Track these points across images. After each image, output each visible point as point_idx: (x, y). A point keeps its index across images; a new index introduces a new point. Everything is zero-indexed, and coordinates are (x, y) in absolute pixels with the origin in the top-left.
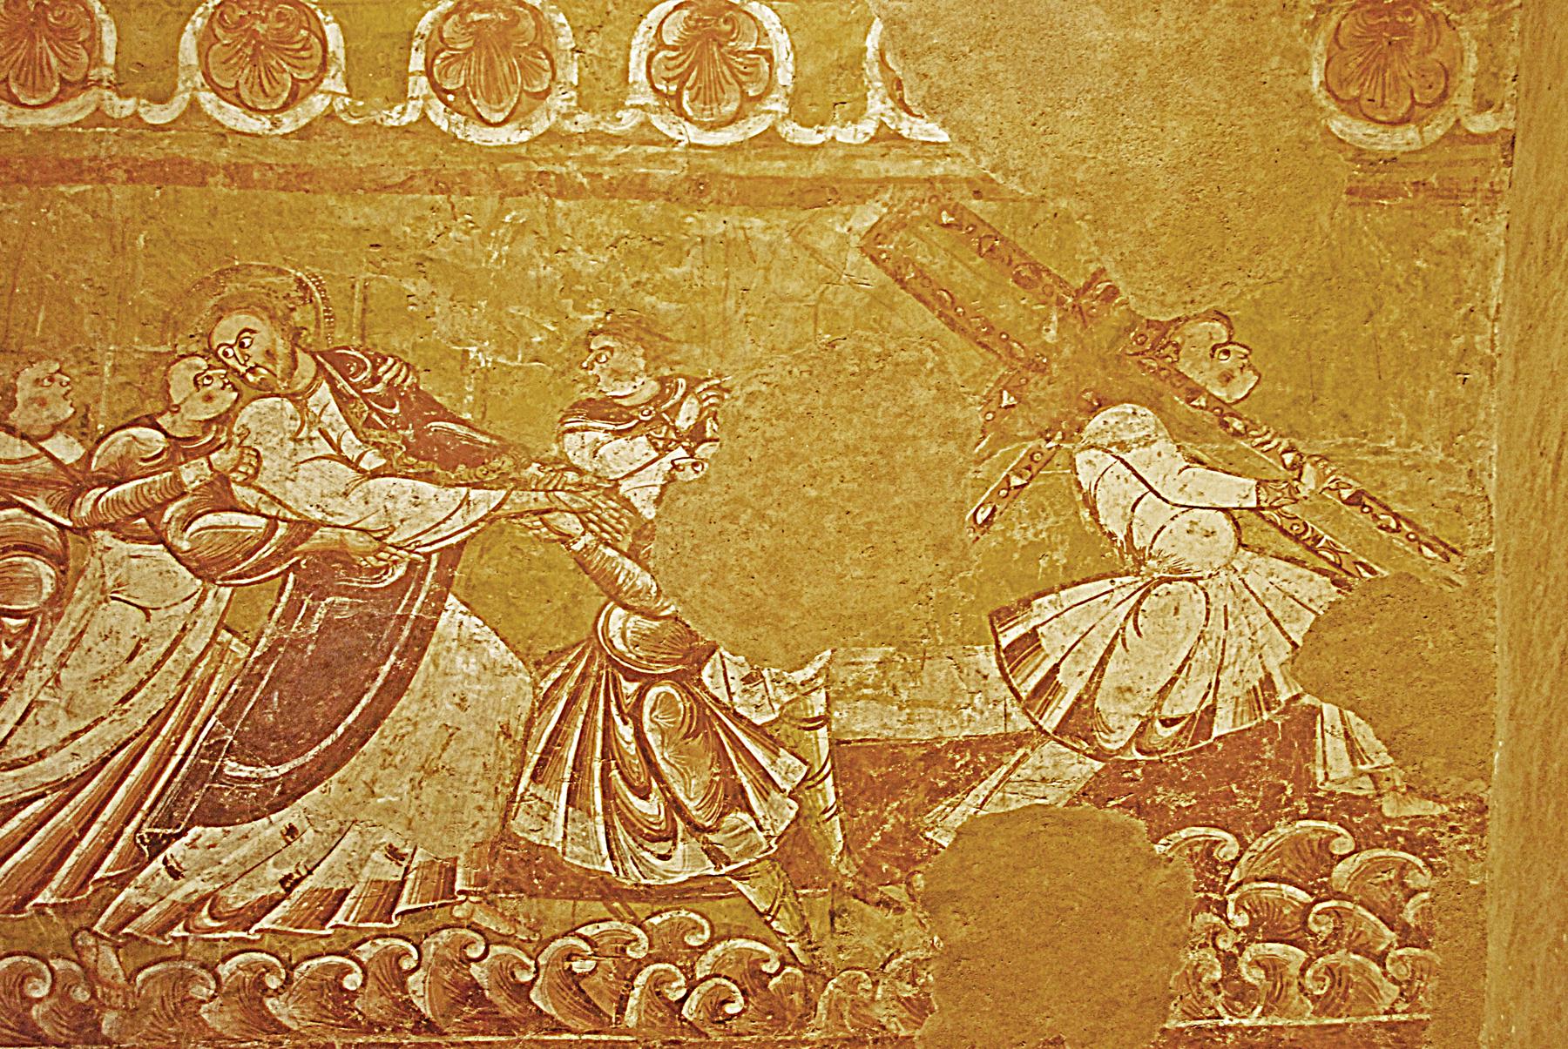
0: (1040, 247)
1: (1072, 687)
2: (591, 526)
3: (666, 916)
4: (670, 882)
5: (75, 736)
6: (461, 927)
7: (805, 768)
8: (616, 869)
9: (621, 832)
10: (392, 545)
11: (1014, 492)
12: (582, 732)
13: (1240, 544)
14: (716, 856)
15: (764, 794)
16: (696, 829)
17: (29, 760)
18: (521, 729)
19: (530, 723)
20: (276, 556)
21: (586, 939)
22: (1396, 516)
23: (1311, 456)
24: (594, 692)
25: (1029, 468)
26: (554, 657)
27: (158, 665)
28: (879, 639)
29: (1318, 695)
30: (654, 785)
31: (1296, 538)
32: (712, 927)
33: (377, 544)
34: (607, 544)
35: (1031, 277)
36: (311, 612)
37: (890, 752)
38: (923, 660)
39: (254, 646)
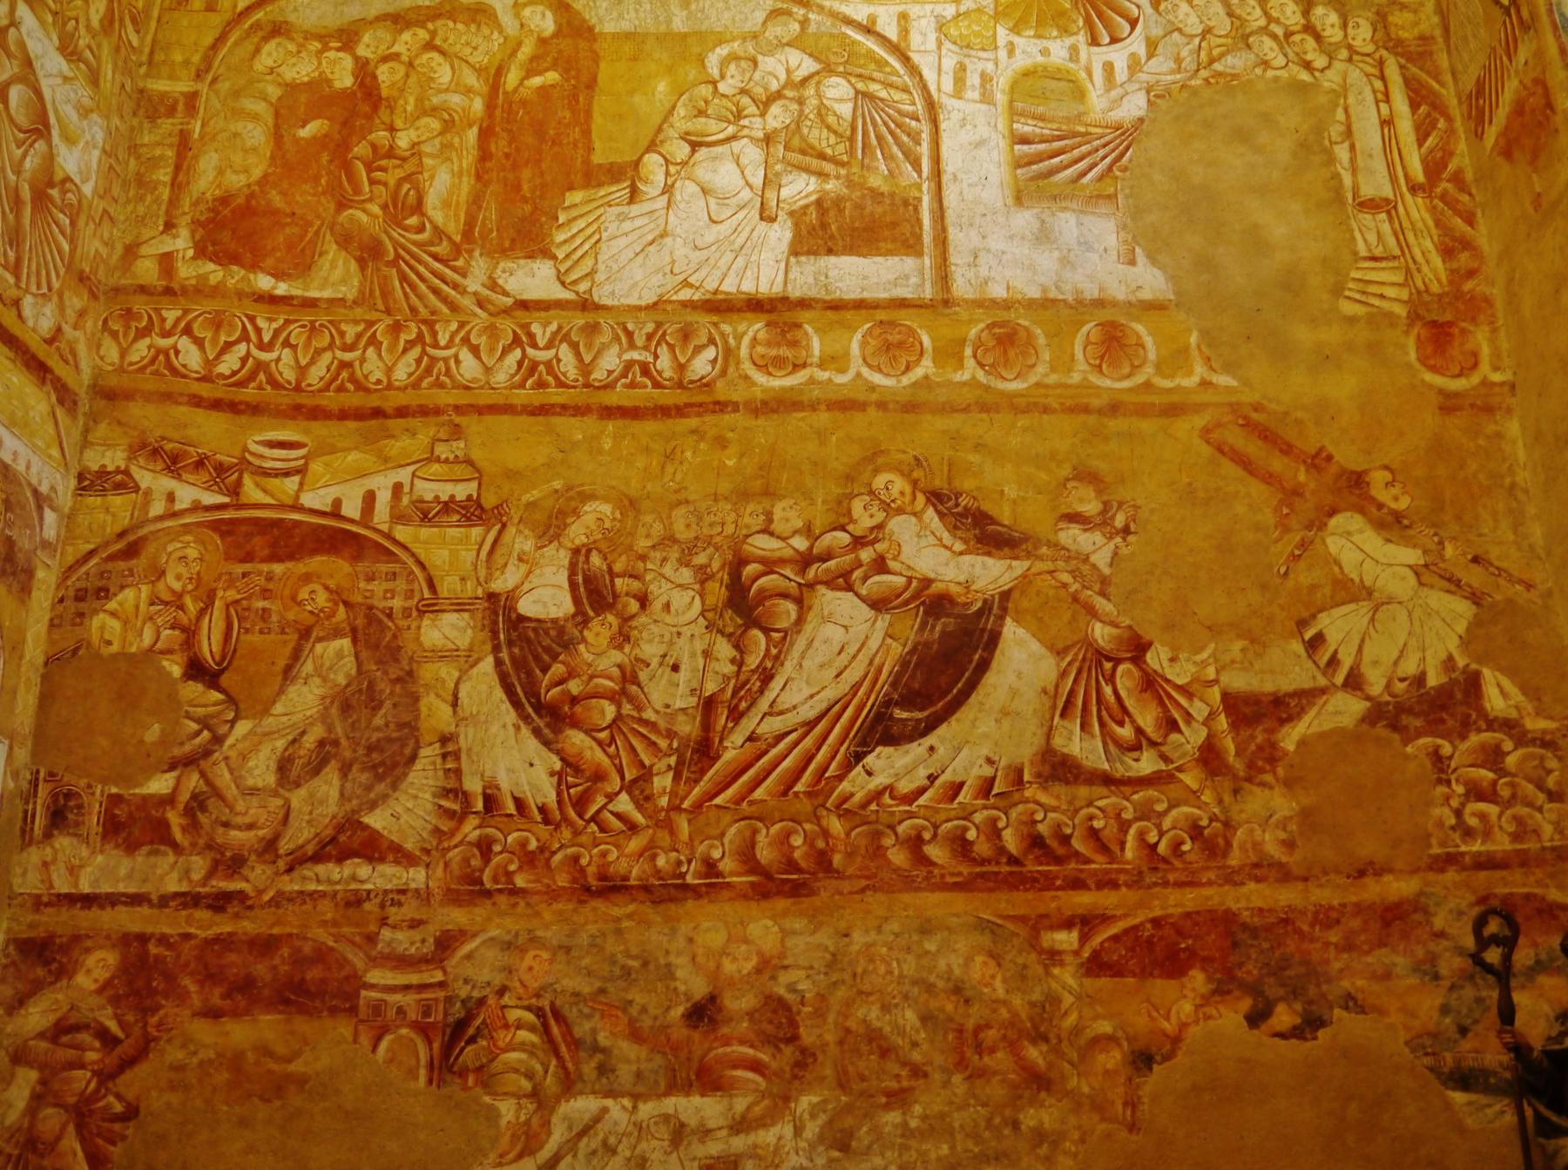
0: (1290, 434)
1: (1347, 661)
5: (812, 696)
9: (1112, 748)
13: (1421, 584)
14: (1165, 759)
16: (1153, 744)
17: (788, 711)
19: (1057, 686)
20: (913, 598)
27: (854, 657)
28: (1240, 636)
29: (1479, 660)
31: (1449, 580)
35: (1287, 449)
36: (933, 627)
37: (1253, 700)
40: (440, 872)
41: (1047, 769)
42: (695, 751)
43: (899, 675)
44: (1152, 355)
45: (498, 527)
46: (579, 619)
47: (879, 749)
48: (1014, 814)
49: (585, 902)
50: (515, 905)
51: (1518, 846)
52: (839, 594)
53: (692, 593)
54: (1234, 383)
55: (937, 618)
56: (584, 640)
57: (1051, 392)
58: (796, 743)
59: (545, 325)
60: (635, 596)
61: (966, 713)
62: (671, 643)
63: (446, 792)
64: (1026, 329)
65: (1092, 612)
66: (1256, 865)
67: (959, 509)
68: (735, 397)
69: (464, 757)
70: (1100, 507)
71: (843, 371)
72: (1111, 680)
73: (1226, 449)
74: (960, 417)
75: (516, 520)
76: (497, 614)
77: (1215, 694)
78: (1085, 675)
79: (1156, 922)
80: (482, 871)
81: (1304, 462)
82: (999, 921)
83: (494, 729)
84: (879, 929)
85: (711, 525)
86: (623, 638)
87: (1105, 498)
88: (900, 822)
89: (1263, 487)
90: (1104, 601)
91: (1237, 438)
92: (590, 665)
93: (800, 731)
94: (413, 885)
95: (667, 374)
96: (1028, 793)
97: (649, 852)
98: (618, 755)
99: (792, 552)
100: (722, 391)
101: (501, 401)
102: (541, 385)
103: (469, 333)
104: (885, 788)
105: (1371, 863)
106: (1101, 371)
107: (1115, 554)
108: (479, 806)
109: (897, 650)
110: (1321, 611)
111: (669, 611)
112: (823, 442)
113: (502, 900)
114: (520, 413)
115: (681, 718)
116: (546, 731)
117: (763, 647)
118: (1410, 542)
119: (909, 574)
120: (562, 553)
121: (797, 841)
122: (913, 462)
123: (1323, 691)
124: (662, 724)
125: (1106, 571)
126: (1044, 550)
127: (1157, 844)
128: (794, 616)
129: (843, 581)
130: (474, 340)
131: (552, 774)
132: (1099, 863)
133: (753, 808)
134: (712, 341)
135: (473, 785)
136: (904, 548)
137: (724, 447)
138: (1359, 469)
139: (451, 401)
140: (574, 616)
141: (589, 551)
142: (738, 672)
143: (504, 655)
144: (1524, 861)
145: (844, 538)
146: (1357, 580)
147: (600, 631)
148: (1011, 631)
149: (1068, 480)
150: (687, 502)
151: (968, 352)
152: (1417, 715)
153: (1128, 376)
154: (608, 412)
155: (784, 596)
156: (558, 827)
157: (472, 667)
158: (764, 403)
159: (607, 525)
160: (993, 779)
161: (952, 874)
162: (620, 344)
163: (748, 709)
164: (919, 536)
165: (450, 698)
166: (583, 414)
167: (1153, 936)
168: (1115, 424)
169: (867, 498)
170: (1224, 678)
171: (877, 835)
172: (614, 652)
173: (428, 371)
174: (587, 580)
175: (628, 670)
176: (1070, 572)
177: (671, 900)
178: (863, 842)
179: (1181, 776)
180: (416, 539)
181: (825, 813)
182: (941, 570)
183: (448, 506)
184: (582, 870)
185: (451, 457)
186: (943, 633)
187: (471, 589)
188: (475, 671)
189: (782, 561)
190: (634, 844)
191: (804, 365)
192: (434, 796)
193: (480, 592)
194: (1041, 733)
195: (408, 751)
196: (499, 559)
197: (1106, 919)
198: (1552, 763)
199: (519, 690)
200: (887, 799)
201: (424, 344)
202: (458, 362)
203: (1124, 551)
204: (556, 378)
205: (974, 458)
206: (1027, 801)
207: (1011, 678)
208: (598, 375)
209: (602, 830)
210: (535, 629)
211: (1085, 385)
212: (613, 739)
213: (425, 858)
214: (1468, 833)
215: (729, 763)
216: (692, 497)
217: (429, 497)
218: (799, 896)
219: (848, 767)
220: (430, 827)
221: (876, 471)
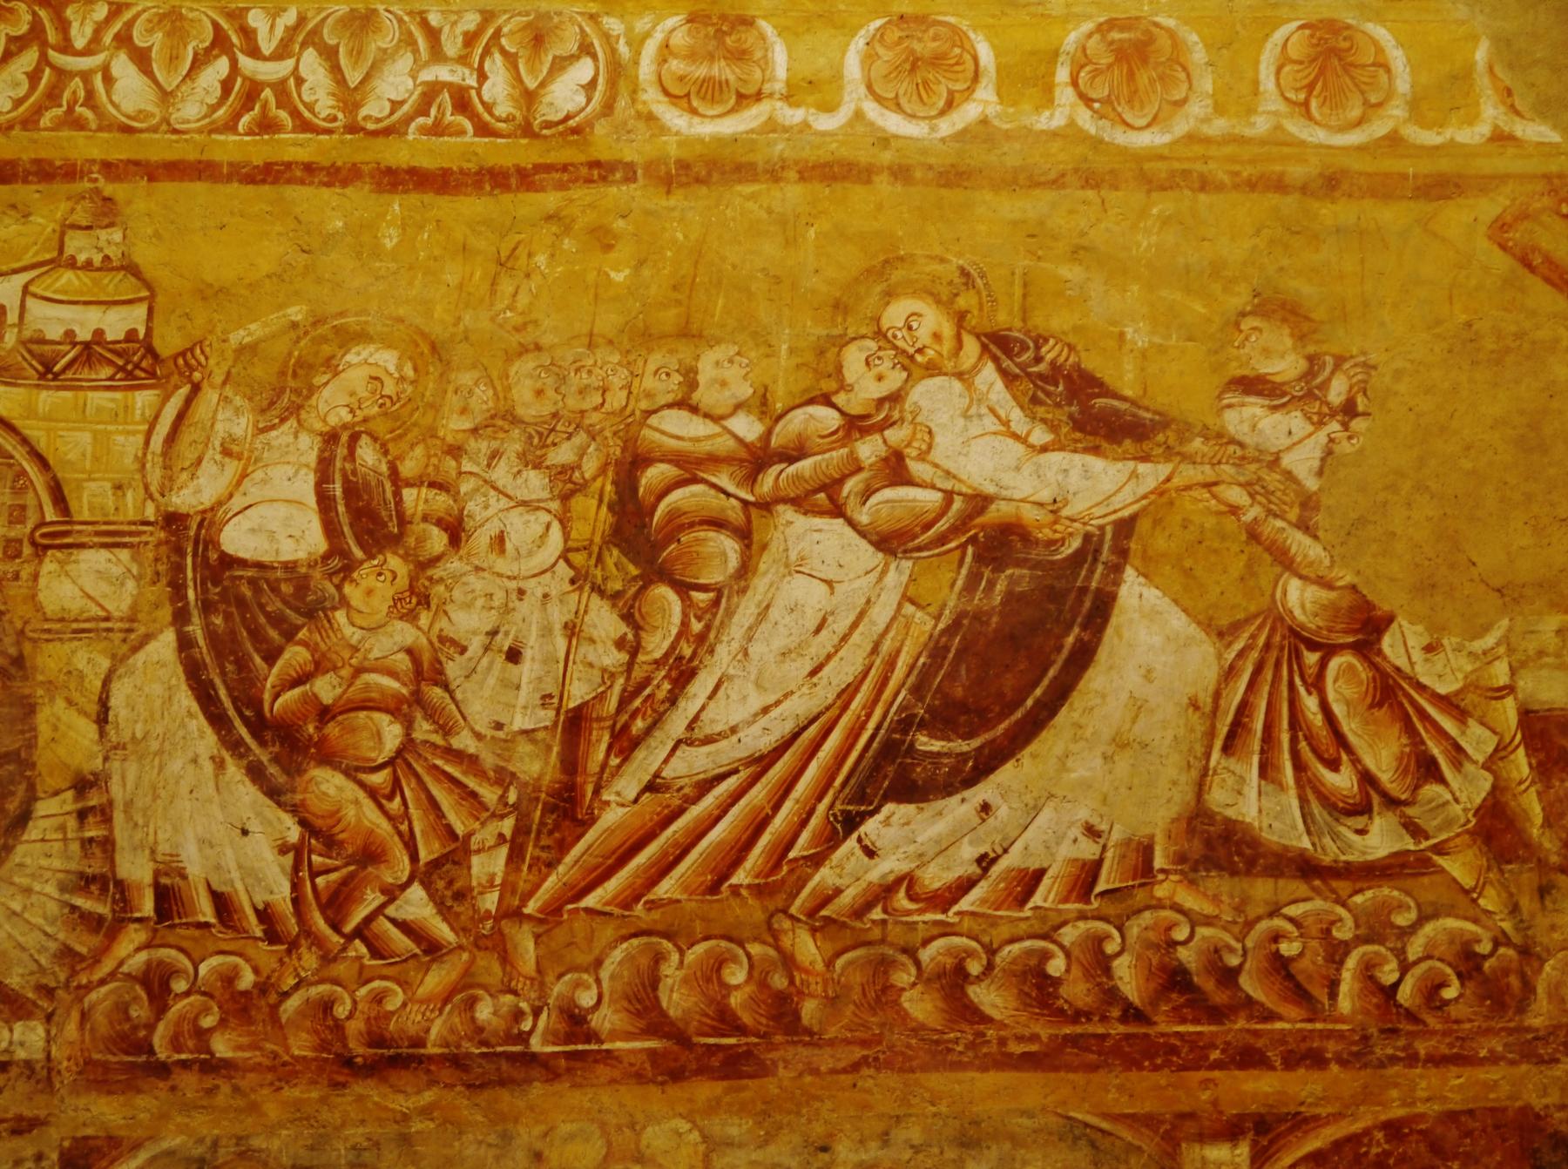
2: (1259, 498)
3: (1369, 894)
4: (1369, 858)
5: (766, 710)
6: (1163, 907)
7: (1495, 739)
8: (1314, 844)
9: (1316, 808)
10: (1067, 518)
14: (1415, 830)
15: (1457, 765)
16: (1391, 802)
17: (721, 736)
18: (1209, 700)
19: (1217, 696)
20: (955, 530)
21: (1291, 920)
24: (1278, 665)
26: (1236, 628)
27: (845, 638)
30: (1344, 757)
32: (1419, 906)
33: (1051, 517)
34: (1276, 516)
36: (991, 584)
39: (938, 618)
40: (71, 1029)
41: (1196, 848)
42: (549, 809)
43: (926, 676)
44: (1403, 85)
45: (185, 390)
46: (336, 563)
47: (889, 808)
48: (1134, 929)
49: (344, 1085)
50: (211, 1091)
52: (818, 522)
53: (545, 517)
54: (1555, 137)
55: (999, 569)
56: (344, 602)
57: (1213, 151)
58: (736, 796)
59: (275, 14)
60: (439, 523)
61: (1050, 743)
62: (507, 610)
63: (85, 882)
64: (1171, 33)
65: (1285, 561)
67: (1042, 368)
68: (629, 155)
69: (118, 817)
70: (1302, 365)
71: (829, 108)
72: (1317, 684)
73: (1537, 260)
74: (1048, 195)
75: (218, 378)
76: (181, 552)
77: (1508, 712)
78: (1268, 674)
79: (1393, 1129)
80: (151, 1027)
82: (1105, 1125)
83: (176, 765)
84: (885, 1139)
85: (583, 391)
86: (416, 598)
87: (1311, 349)
88: (926, 942)
92: (356, 649)
93: (744, 774)
94: (21, 1054)
95: (502, 110)
96: (1161, 891)
97: (463, 993)
98: (406, 815)
99: (731, 443)
100: (603, 143)
101: (192, 155)
102: (267, 126)
103: (129, 25)
104: (899, 881)
106: (1308, 116)
107: (1329, 452)
108: (147, 907)
109: (923, 625)
111: (502, 551)
112: (790, 242)
113: (189, 1082)
114: (229, 178)
115: (524, 747)
116: (273, 770)
117: (677, 618)
119: (948, 485)
120: (305, 440)
121: (736, 975)
122: (958, 280)
124: (489, 760)
125: (1312, 484)
126: (1197, 443)
127: (1396, 985)
128: (734, 562)
129: (825, 497)
130: (139, 40)
131: (283, 850)
132: (1291, 1020)
133: (656, 915)
134: (586, 49)
135: (136, 869)
136: (938, 439)
137: (608, 248)
139: (96, 153)
140: (326, 557)
141: (355, 438)
142: (630, 666)
143: (196, 629)
145: (828, 418)
147: (375, 585)
148: (1134, 592)
149: (1243, 314)
150: (538, 348)
151: (1062, 74)
153: (1359, 123)
154: (393, 179)
155: (718, 524)
156: (293, 946)
157: (135, 650)
158: (684, 166)
159: (390, 389)
160: (1099, 863)
161: (1020, 1039)
162: (416, 51)
163: (648, 731)
164: (966, 415)
165: (93, 708)
166: (345, 183)
167: (1387, 1154)
168: (1333, 212)
169: (873, 345)
170: (1525, 683)
171: (883, 966)
172: (399, 625)
173: (53, 96)
174: (351, 491)
175: (426, 658)
176: (1245, 485)
177: (503, 1083)
178: (857, 978)
179: (1440, 861)
180: (31, 412)
181: (787, 924)
182: (1008, 479)
183: (90, 351)
184: (338, 1027)
185: (97, 259)
186: (1009, 596)
187: (132, 506)
188: (141, 656)
189: (714, 460)
190: (435, 980)
191: (758, 96)
192: (63, 888)
193: (150, 512)
194: (1187, 780)
195: (12, 806)
196: (186, 449)
197: (1301, 1122)
199: (223, 693)
200: (901, 900)
201: (44, 44)
202: (108, 80)
203: (1345, 447)
204: (295, 114)
205: (1071, 272)
206: (1159, 905)
207: (1132, 679)
208: (374, 109)
209: (376, 953)
210: (252, 582)
211: (1278, 139)
212: (396, 786)
213: (44, 1003)
215: (610, 831)
216: (546, 340)
217: (55, 333)
218: (741, 1076)
219: (831, 840)
220: (53, 946)
221: (889, 295)
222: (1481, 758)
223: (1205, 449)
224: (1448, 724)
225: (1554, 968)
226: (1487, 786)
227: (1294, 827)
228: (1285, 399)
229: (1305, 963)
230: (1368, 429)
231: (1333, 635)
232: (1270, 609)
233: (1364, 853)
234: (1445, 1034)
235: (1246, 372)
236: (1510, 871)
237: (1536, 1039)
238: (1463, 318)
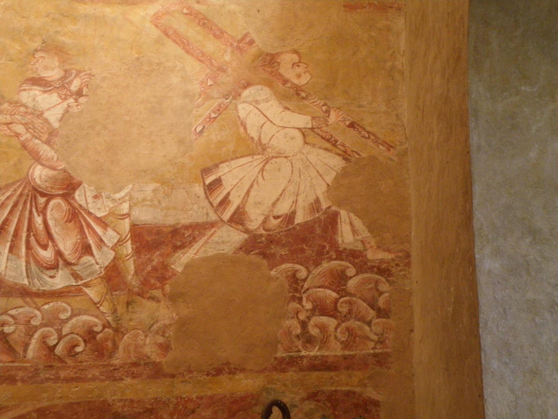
3: (51, 304)
4: (54, 288)
7: (119, 237)
8: (29, 282)
9: (33, 267)
11: (212, 120)
12: (19, 220)
13: (306, 143)
14: (76, 276)
15: (99, 247)
16: (68, 264)
21: (12, 316)
22: (368, 132)
23: (333, 108)
24: (25, 203)
25: (219, 110)
30: (50, 244)
31: (328, 141)
32: (72, 310)
34: (36, 138)
38: (172, 189)
51: (347, 353)
65: (37, 158)
66: (135, 364)
70: (62, 73)
72: (43, 212)
73: (171, 32)
78: (20, 207)
81: (231, 45)
87: (67, 67)
89: (196, 64)
90: (45, 147)
91: (181, 25)
105: (228, 364)
107: (67, 111)
110: (222, 162)
118: (301, 111)
123: (213, 225)
125: (56, 125)
126: (6, 106)
127: (55, 346)
138: (273, 52)
144: (348, 364)
146: (256, 139)
149: (36, 51)
152: (284, 246)
176: (25, 124)
179: (87, 290)
198: (384, 287)
203: (75, 110)
214: (309, 341)
222: (111, 245)
223: (9, 108)
224: (99, 230)
225: (128, 338)
226: (112, 257)
227: (22, 274)
228: (51, 88)
229: (15, 336)
230: (86, 102)
231: (53, 190)
232: (25, 178)
233: (52, 286)
234: (74, 368)
235: (34, 76)
236: (116, 295)
237: (114, 370)
238: (137, 56)
